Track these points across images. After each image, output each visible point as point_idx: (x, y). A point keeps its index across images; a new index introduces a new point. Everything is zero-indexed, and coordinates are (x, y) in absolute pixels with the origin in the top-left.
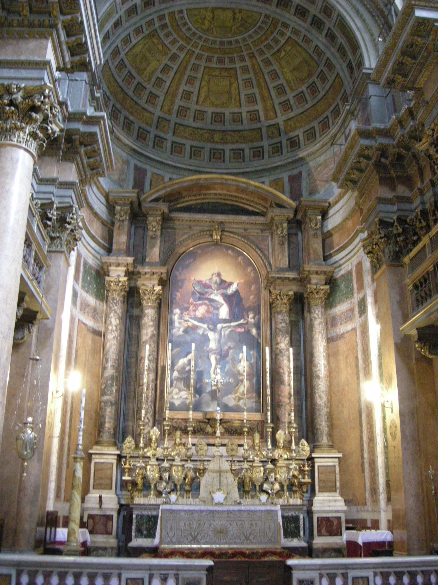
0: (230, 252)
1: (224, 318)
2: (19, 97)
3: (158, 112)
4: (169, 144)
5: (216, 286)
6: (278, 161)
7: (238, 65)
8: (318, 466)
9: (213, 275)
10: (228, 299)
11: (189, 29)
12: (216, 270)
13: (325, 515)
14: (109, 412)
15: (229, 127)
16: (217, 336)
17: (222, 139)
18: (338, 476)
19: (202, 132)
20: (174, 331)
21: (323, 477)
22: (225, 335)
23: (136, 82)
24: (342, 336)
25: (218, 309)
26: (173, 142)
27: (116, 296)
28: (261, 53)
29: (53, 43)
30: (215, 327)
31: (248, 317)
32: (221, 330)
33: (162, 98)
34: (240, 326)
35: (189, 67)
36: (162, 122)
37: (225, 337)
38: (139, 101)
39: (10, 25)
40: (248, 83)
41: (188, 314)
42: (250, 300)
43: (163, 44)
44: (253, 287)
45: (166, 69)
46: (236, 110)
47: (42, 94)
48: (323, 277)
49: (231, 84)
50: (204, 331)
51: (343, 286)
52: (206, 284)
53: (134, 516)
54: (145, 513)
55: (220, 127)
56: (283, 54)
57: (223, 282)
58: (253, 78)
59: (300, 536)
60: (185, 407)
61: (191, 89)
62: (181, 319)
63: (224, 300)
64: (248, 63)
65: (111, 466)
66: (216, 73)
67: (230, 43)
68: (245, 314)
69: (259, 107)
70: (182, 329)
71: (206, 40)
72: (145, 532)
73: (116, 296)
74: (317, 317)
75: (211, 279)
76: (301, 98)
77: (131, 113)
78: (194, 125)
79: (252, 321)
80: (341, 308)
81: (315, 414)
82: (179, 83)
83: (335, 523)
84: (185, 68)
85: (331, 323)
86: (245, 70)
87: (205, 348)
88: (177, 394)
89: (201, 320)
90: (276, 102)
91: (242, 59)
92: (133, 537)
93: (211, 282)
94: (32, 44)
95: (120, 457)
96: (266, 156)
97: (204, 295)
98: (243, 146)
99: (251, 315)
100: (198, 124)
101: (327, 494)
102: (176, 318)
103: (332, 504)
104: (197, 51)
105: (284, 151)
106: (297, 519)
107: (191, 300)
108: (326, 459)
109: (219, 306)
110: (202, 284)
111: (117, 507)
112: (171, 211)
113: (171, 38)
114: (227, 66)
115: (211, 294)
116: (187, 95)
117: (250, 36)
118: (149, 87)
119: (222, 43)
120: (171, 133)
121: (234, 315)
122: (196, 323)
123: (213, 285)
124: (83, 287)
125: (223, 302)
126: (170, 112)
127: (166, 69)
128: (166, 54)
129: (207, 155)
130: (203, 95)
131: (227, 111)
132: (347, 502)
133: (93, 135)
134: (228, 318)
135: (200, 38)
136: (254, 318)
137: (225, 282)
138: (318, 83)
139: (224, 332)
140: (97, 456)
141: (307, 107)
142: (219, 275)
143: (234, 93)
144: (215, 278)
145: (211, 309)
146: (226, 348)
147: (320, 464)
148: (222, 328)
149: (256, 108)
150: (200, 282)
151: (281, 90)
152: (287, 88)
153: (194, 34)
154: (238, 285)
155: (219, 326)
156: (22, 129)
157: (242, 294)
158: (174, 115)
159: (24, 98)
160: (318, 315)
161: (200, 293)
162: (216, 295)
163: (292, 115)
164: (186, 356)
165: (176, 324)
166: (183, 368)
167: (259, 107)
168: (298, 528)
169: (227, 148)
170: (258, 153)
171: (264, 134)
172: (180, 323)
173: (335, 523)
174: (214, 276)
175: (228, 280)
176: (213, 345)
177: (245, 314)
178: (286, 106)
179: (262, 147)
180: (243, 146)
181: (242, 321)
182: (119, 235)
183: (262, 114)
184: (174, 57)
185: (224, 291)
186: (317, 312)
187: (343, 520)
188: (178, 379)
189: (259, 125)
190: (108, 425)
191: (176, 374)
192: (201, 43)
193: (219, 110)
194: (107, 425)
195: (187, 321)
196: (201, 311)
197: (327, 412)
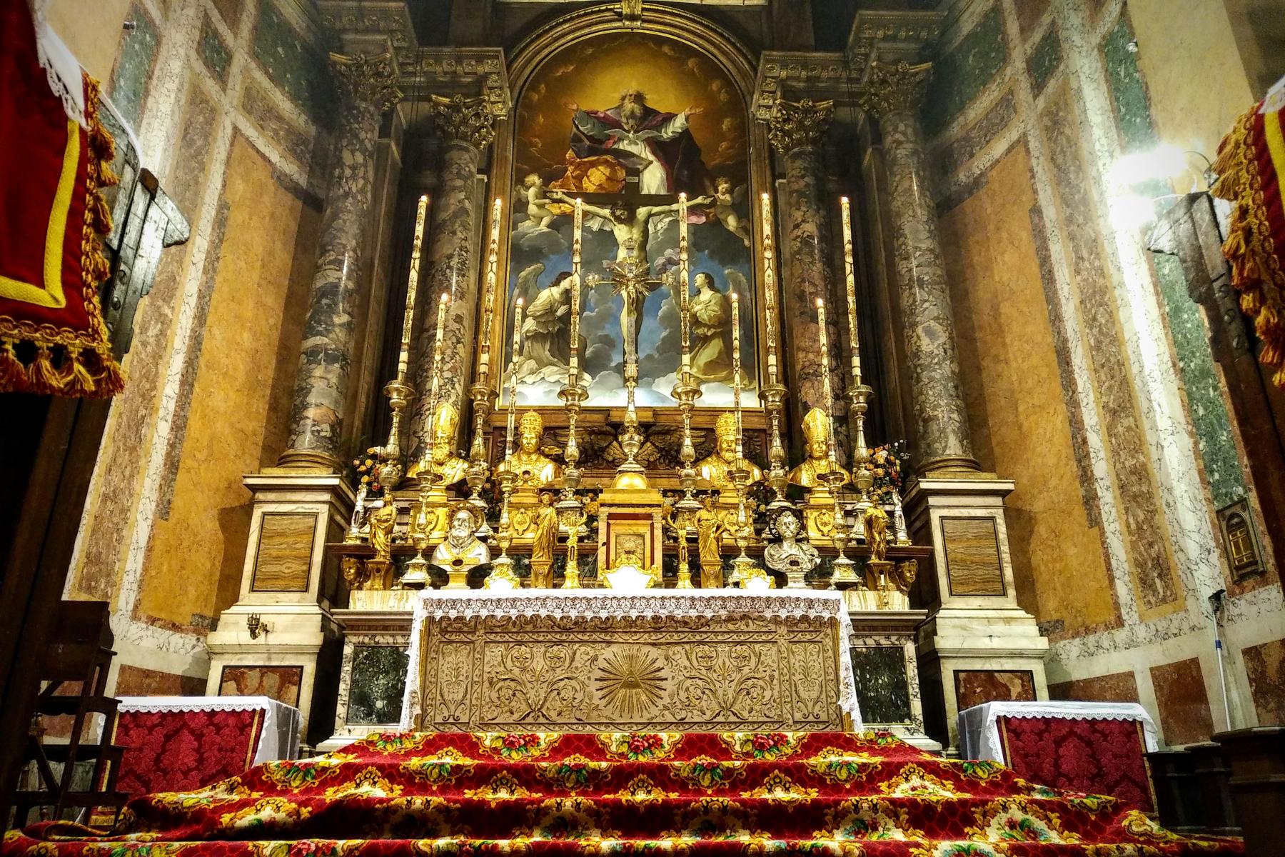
0: (666, 49)
1: (653, 192)
5: (631, 122)
8: (942, 518)
9: (623, 98)
10: (661, 149)
12: (633, 88)
13: (978, 665)
16: (636, 234)
18: (1005, 548)
21: (958, 549)
22: (656, 232)
25: (637, 173)
31: (717, 191)
32: (646, 222)
37: (656, 238)
41: (561, 187)
42: (718, 152)
44: (726, 124)
50: (603, 225)
52: (606, 118)
53: (348, 650)
57: (648, 113)
59: (909, 716)
62: (546, 197)
63: (654, 153)
65: (311, 521)
68: (707, 183)
70: (545, 221)
72: (379, 704)
74: (902, 138)
75: (620, 107)
79: (728, 197)
81: (919, 380)
87: (605, 263)
88: (532, 373)
92: (338, 722)
93: (619, 114)
97: (601, 142)
101: (976, 602)
103: (999, 628)
107: (570, 154)
109: (641, 167)
110: (598, 118)
115: (621, 139)
123: (624, 120)
125: (651, 157)
134: (663, 192)
136: (730, 191)
137: (656, 113)
139: (656, 226)
140: (271, 496)
142: (639, 98)
144: (629, 106)
145: (621, 174)
147: (945, 512)
148: (650, 215)
150: (591, 115)
154: (687, 119)
155: (642, 212)
157: (698, 138)
160: (904, 134)
161: (590, 138)
162: (631, 142)
164: (557, 283)
165: (532, 209)
166: (551, 310)
168: (900, 686)
172: (541, 206)
174: (626, 101)
175: (663, 110)
177: (707, 183)
185: (654, 133)
186: (902, 127)
188: (535, 337)
195: (560, 201)
196: (596, 178)
197: (953, 372)
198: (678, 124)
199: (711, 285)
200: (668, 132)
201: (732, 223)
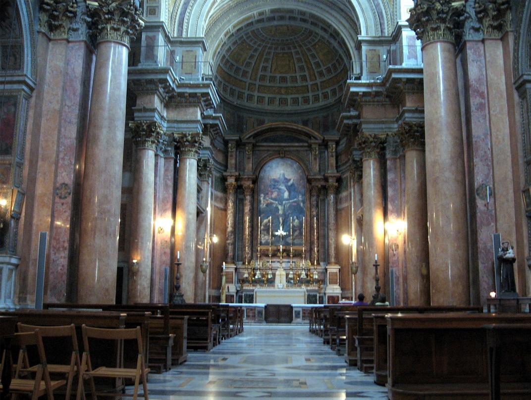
2: (189, 138)
3: (248, 81)
4: (256, 98)
7: (293, 51)
11: (263, 36)
12: (282, 172)
14: (230, 248)
15: (289, 84)
16: (283, 208)
17: (286, 92)
19: (274, 88)
20: (261, 206)
21: (331, 277)
23: (235, 67)
24: (343, 209)
26: (258, 97)
27: (231, 191)
28: (306, 45)
29: (200, 110)
30: (282, 203)
33: (250, 72)
34: (294, 202)
35: (265, 54)
36: (251, 87)
38: (237, 77)
39: (182, 102)
43: (249, 45)
45: (252, 57)
46: (294, 75)
47: (199, 136)
48: (335, 179)
49: (289, 61)
51: (345, 183)
54: (248, 293)
55: (284, 85)
56: (317, 46)
57: (286, 179)
58: (302, 57)
60: (267, 244)
61: (267, 65)
64: (298, 49)
66: (281, 55)
67: (287, 40)
69: (307, 73)
71: (274, 40)
73: (231, 191)
77: (234, 85)
78: (269, 85)
80: (344, 194)
82: (259, 65)
83: (336, 299)
84: (262, 55)
85: (337, 201)
86: (297, 53)
89: (275, 199)
90: (316, 71)
91: (295, 48)
94: (191, 110)
95: (236, 269)
96: (311, 103)
98: (297, 96)
99: (300, 196)
100: (272, 84)
102: (262, 198)
104: (269, 45)
105: (321, 100)
106: (316, 296)
108: (333, 269)
111: (236, 291)
112: (256, 142)
114: (286, 51)
116: (265, 69)
117: (298, 37)
118: (243, 68)
120: (256, 91)
121: (290, 198)
122: (272, 201)
124: (215, 189)
125: (285, 189)
126: (255, 80)
127: (252, 57)
129: (277, 103)
130: (274, 68)
131: (288, 76)
132: (342, 289)
133: (217, 125)
135: (270, 39)
138: (337, 65)
141: (332, 76)
146: (287, 213)
151: (318, 65)
152: (321, 64)
153: (266, 38)
156: (192, 151)
157: (296, 185)
158: (258, 81)
159: (192, 138)
163: (324, 79)
165: (262, 202)
166: (266, 224)
167: (307, 73)
168: (316, 300)
169: (289, 97)
171: (310, 89)
173: (336, 299)
176: (281, 212)
178: (321, 74)
179: (309, 97)
180: (297, 96)
181: (295, 200)
182: (231, 159)
183: (308, 77)
184: (256, 50)
187: (340, 297)
188: (264, 230)
190: (231, 254)
191: (262, 227)
192: (271, 41)
193: (284, 75)
194: (230, 254)
196: (275, 195)
198: (291, 182)
199: (297, 219)
200: (290, 184)
201: (302, 205)
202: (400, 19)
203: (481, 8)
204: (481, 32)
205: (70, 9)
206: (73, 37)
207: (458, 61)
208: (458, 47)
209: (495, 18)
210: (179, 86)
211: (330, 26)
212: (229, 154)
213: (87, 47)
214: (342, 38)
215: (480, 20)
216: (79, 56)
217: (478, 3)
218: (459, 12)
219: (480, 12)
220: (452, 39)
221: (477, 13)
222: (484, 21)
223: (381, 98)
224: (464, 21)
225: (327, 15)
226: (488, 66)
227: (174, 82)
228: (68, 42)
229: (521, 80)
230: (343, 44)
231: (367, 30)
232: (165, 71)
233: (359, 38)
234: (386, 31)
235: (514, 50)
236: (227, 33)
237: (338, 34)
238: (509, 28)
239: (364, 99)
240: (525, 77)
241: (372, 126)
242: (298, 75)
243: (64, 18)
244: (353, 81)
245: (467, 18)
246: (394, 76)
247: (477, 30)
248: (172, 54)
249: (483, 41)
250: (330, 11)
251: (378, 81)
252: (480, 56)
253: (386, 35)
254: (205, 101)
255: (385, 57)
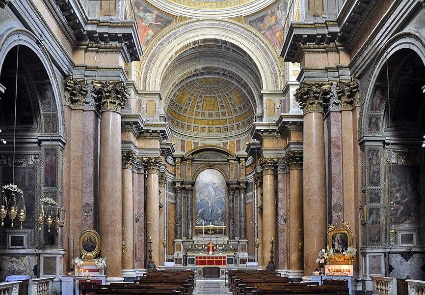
6: (233, 133)
28: (226, 91)
40: (221, 101)
45: (189, 99)
66: (209, 98)
69: (226, 110)
76: (240, 108)
86: (220, 97)
90: (232, 109)
91: (218, 93)
96: (229, 131)
98: (220, 126)
113: (191, 89)
118: (184, 107)
119: (210, 88)
127: (189, 99)
128: (189, 94)
130: (204, 107)
131: (214, 112)
143: (216, 105)
149: (224, 111)
151: (233, 105)
153: (199, 86)
163: (238, 115)
167: (226, 110)
169: (214, 127)
170: (226, 129)
178: (235, 111)
180: (220, 126)
189: (226, 118)
202: (289, 80)
203: (340, 90)
204: (340, 105)
205: (84, 89)
206: (87, 107)
207: (325, 122)
208: (326, 114)
209: (349, 97)
210: (146, 125)
211: (242, 79)
212: (177, 166)
213: (95, 113)
214: (250, 88)
215: (340, 98)
216: (91, 120)
217: (339, 87)
218: (326, 93)
219: (340, 93)
220: (321, 109)
221: (338, 93)
222: (342, 98)
223: (275, 133)
224: (330, 98)
225: (240, 72)
226: (343, 128)
227: (142, 123)
228: (84, 111)
229: (362, 140)
230: (250, 92)
231: (267, 86)
232: (137, 116)
233: (262, 92)
234: (279, 86)
235: (359, 119)
236: (174, 84)
237: (247, 85)
238: (357, 104)
239: (264, 134)
240: (365, 138)
241: (269, 152)
242: (220, 111)
243: (80, 95)
244: (258, 122)
245: (332, 96)
246: (284, 120)
247: (337, 104)
248: (140, 101)
249: (341, 112)
250: (242, 69)
251: (274, 123)
252: (338, 121)
253: (279, 90)
254: (162, 135)
255: (278, 106)
